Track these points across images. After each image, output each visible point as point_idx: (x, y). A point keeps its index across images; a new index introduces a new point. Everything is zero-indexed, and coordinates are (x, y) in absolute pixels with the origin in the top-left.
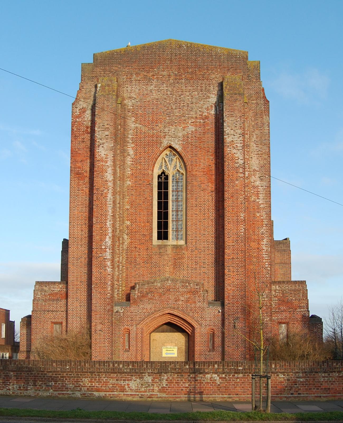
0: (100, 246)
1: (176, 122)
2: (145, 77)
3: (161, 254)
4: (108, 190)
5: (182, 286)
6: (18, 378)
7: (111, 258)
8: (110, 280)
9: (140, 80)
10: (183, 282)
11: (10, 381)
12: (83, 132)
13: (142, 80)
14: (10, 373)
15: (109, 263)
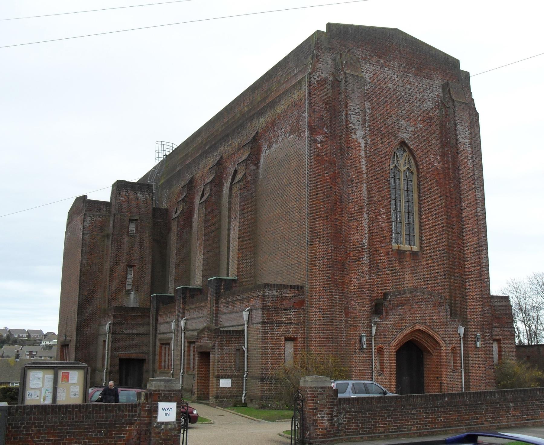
0: (357, 248)
1: (407, 116)
2: (378, 62)
3: (400, 260)
4: (362, 183)
5: (428, 299)
6: (516, 408)
7: (368, 262)
8: (368, 289)
9: (374, 64)
10: (429, 295)
11: (510, 413)
12: (322, 108)
13: (376, 65)
14: (510, 404)
15: (366, 269)
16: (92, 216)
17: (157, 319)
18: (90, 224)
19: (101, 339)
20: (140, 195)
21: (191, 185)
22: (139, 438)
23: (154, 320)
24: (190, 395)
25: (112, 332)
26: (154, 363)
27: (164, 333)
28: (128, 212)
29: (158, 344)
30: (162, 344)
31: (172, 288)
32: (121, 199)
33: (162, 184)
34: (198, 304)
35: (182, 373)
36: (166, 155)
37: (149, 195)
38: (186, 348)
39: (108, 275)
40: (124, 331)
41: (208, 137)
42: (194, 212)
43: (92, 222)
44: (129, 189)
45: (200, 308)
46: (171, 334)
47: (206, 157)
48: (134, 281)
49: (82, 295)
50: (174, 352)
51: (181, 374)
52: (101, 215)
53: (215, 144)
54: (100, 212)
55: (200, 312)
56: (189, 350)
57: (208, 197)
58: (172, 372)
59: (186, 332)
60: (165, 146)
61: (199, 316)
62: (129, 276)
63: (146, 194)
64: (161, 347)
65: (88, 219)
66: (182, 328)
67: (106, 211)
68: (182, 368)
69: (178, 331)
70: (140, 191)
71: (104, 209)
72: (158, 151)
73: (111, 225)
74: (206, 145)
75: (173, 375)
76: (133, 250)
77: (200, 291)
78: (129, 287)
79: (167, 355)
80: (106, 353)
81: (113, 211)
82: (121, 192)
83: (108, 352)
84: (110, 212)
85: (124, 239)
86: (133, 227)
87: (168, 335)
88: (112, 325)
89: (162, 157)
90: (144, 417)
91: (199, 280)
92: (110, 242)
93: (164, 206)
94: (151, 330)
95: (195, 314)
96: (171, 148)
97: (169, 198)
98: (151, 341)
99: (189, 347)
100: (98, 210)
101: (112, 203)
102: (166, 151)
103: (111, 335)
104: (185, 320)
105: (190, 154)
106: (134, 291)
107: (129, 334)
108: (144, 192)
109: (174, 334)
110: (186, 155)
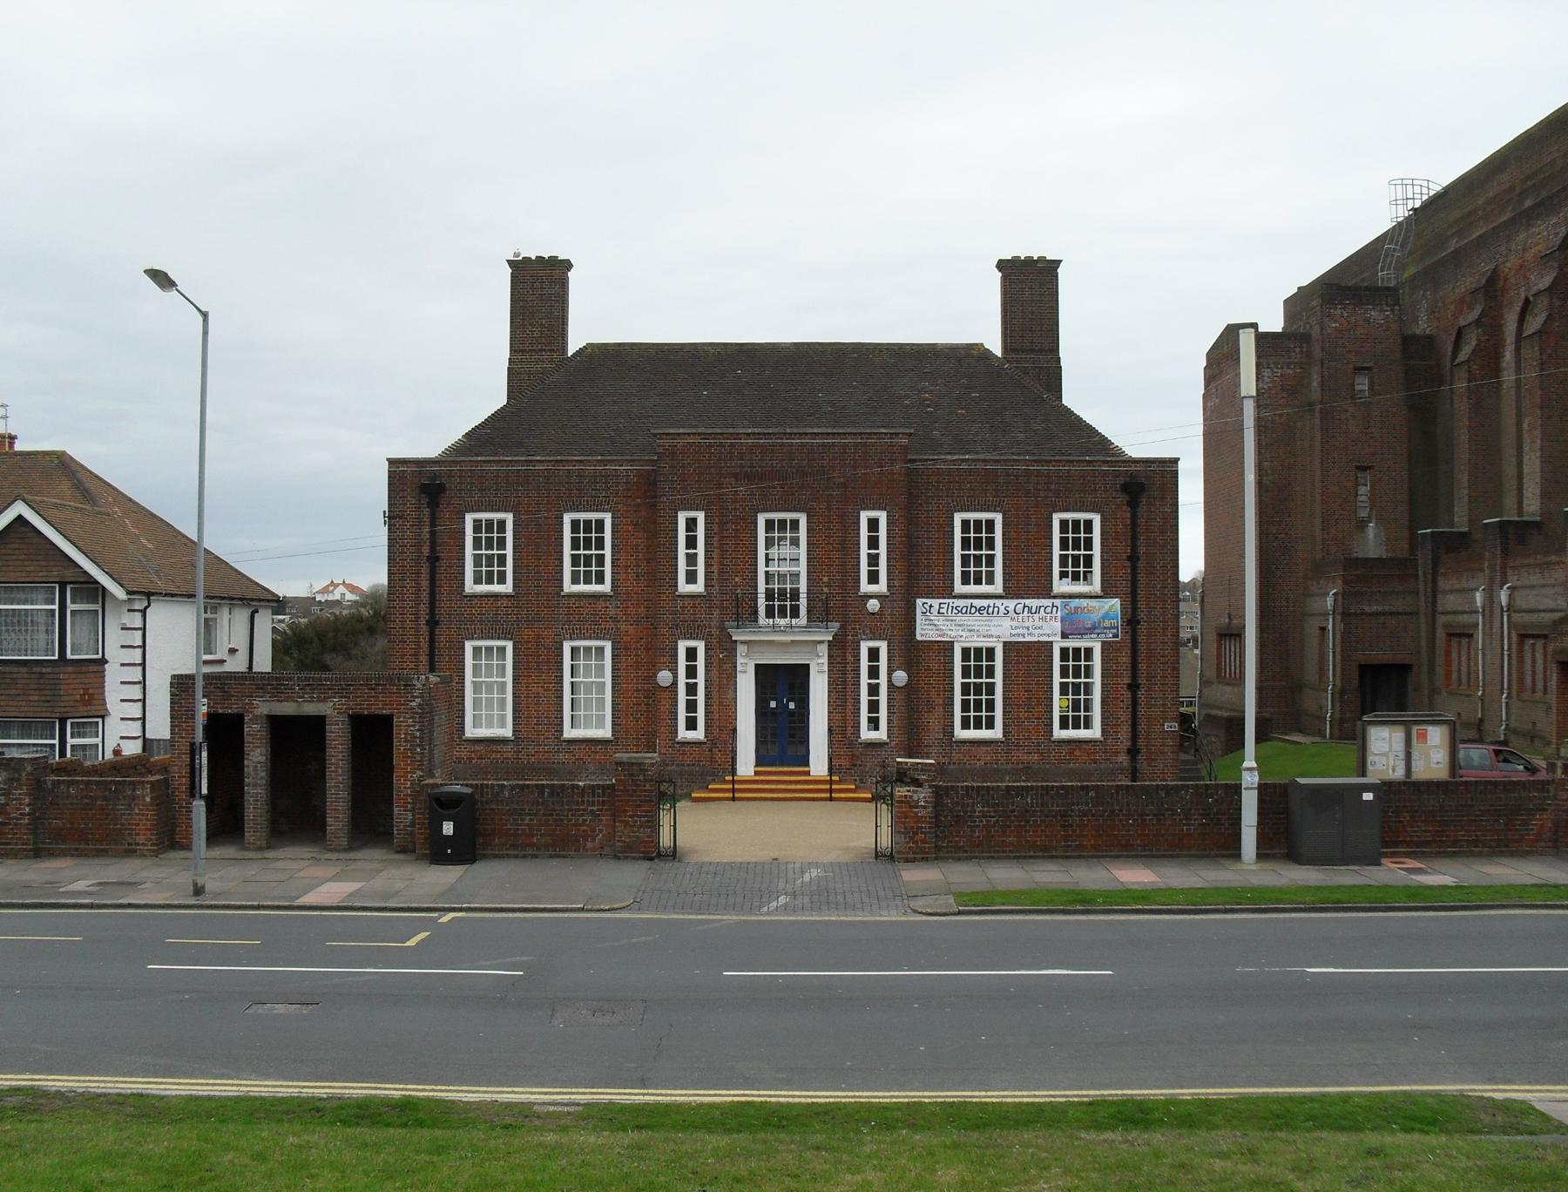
16: (1272, 366)
17: (1435, 582)
18: (1270, 385)
19: (1311, 627)
20: (1373, 313)
21: (1492, 288)
22: (1557, 831)
23: (1430, 585)
24: (1529, 743)
25: (1341, 611)
26: (1432, 671)
27: (1454, 613)
28: (1349, 352)
29: (1440, 634)
30: (1450, 635)
31: (1463, 513)
32: (1334, 325)
33: (1413, 277)
34: (1539, 557)
35: (1507, 698)
36: (1415, 210)
37: (1392, 310)
38: (1514, 646)
39: (1318, 491)
40: (1367, 609)
41: (1528, 178)
42: (1504, 346)
43: (1275, 378)
44: (1348, 302)
45: (1544, 566)
46: (1474, 615)
47: (1528, 225)
48: (1373, 497)
49: (1267, 534)
50: (1483, 654)
51: (1503, 700)
52: (1292, 363)
53: (1551, 197)
54: (1290, 357)
55: (1546, 575)
56: (1521, 651)
57: (1545, 322)
58: (1480, 693)
59: (1513, 615)
60: (1410, 187)
61: (1543, 582)
62: (1362, 490)
63: (1385, 308)
64: (1450, 640)
65: (1266, 374)
66: (1502, 606)
67: (1301, 352)
68: (1505, 687)
69: (1492, 612)
70: (1372, 305)
71: (1298, 350)
72: (1394, 203)
73: (1315, 384)
74: (1523, 195)
75: (1482, 700)
76: (1366, 434)
77: (1537, 525)
78: (1363, 514)
79: (1464, 658)
80: (1331, 654)
81: (1317, 353)
82: (1332, 311)
83: (1334, 652)
84: (1309, 355)
85: (1346, 411)
86: (1362, 384)
87: (1465, 616)
88: (1340, 597)
89: (1402, 213)
90: (1563, 800)
91: (1533, 502)
92: (1317, 421)
93: (1422, 326)
94: (1422, 604)
95: (1535, 579)
96: (1425, 191)
97: (1434, 312)
98: (1423, 627)
99: (1521, 644)
100: (1284, 353)
101: (1314, 335)
102: (1414, 199)
103: (1338, 618)
104: (1508, 588)
105: (1480, 213)
106: (1374, 521)
107: (1376, 614)
108: (1382, 305)
109: (1483, 616)
110: (1470, 213)
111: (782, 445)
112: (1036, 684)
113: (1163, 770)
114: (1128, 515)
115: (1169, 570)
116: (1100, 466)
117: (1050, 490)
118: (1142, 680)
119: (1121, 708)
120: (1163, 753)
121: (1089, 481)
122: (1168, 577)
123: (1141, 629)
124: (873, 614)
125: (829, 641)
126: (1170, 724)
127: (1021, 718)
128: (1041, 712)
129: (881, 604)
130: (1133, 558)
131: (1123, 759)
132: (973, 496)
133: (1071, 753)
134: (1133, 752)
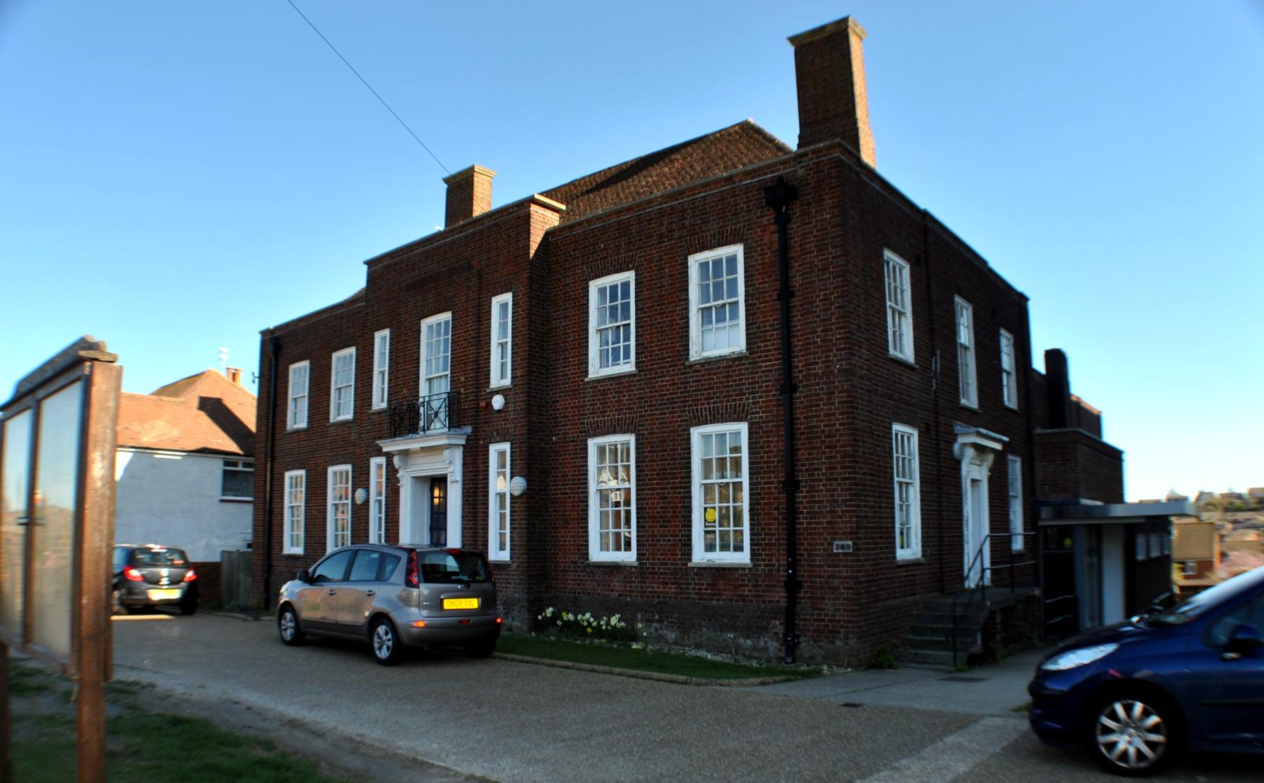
111: (439, 247)
112: (672, 488)
113: (834, 615)
114: (775, 237)
115: (832, 304)
116: (741, 180)
117: (685, 228)
118: (802, 477)
119: (775, 519)
120: (834, 589)
121: (729, 202)
122: (833, 314)
123: (799, 397)
124: (499, 411)
125: (463, 445)
126: (840, 543)
127: (656, 536)
128: (678, 526)
129: (505, 399)
130: (786, 294)
131: (779, 597)
132: (607, 257)
133: (712, 585)
134: (793, 586)
